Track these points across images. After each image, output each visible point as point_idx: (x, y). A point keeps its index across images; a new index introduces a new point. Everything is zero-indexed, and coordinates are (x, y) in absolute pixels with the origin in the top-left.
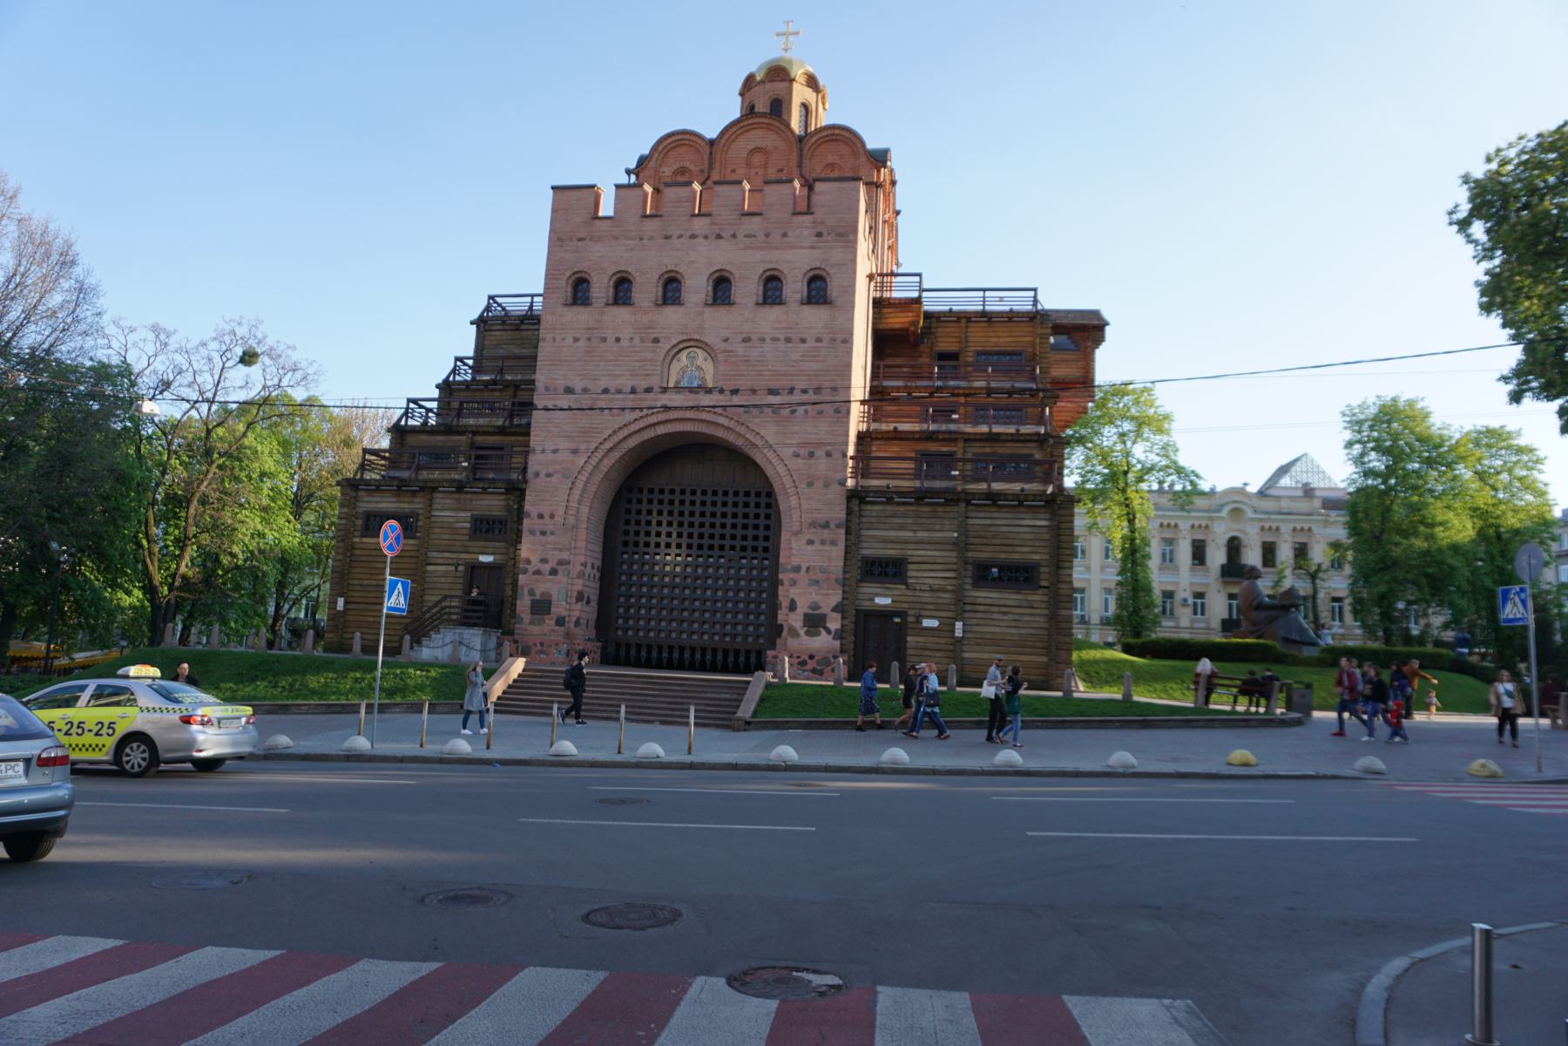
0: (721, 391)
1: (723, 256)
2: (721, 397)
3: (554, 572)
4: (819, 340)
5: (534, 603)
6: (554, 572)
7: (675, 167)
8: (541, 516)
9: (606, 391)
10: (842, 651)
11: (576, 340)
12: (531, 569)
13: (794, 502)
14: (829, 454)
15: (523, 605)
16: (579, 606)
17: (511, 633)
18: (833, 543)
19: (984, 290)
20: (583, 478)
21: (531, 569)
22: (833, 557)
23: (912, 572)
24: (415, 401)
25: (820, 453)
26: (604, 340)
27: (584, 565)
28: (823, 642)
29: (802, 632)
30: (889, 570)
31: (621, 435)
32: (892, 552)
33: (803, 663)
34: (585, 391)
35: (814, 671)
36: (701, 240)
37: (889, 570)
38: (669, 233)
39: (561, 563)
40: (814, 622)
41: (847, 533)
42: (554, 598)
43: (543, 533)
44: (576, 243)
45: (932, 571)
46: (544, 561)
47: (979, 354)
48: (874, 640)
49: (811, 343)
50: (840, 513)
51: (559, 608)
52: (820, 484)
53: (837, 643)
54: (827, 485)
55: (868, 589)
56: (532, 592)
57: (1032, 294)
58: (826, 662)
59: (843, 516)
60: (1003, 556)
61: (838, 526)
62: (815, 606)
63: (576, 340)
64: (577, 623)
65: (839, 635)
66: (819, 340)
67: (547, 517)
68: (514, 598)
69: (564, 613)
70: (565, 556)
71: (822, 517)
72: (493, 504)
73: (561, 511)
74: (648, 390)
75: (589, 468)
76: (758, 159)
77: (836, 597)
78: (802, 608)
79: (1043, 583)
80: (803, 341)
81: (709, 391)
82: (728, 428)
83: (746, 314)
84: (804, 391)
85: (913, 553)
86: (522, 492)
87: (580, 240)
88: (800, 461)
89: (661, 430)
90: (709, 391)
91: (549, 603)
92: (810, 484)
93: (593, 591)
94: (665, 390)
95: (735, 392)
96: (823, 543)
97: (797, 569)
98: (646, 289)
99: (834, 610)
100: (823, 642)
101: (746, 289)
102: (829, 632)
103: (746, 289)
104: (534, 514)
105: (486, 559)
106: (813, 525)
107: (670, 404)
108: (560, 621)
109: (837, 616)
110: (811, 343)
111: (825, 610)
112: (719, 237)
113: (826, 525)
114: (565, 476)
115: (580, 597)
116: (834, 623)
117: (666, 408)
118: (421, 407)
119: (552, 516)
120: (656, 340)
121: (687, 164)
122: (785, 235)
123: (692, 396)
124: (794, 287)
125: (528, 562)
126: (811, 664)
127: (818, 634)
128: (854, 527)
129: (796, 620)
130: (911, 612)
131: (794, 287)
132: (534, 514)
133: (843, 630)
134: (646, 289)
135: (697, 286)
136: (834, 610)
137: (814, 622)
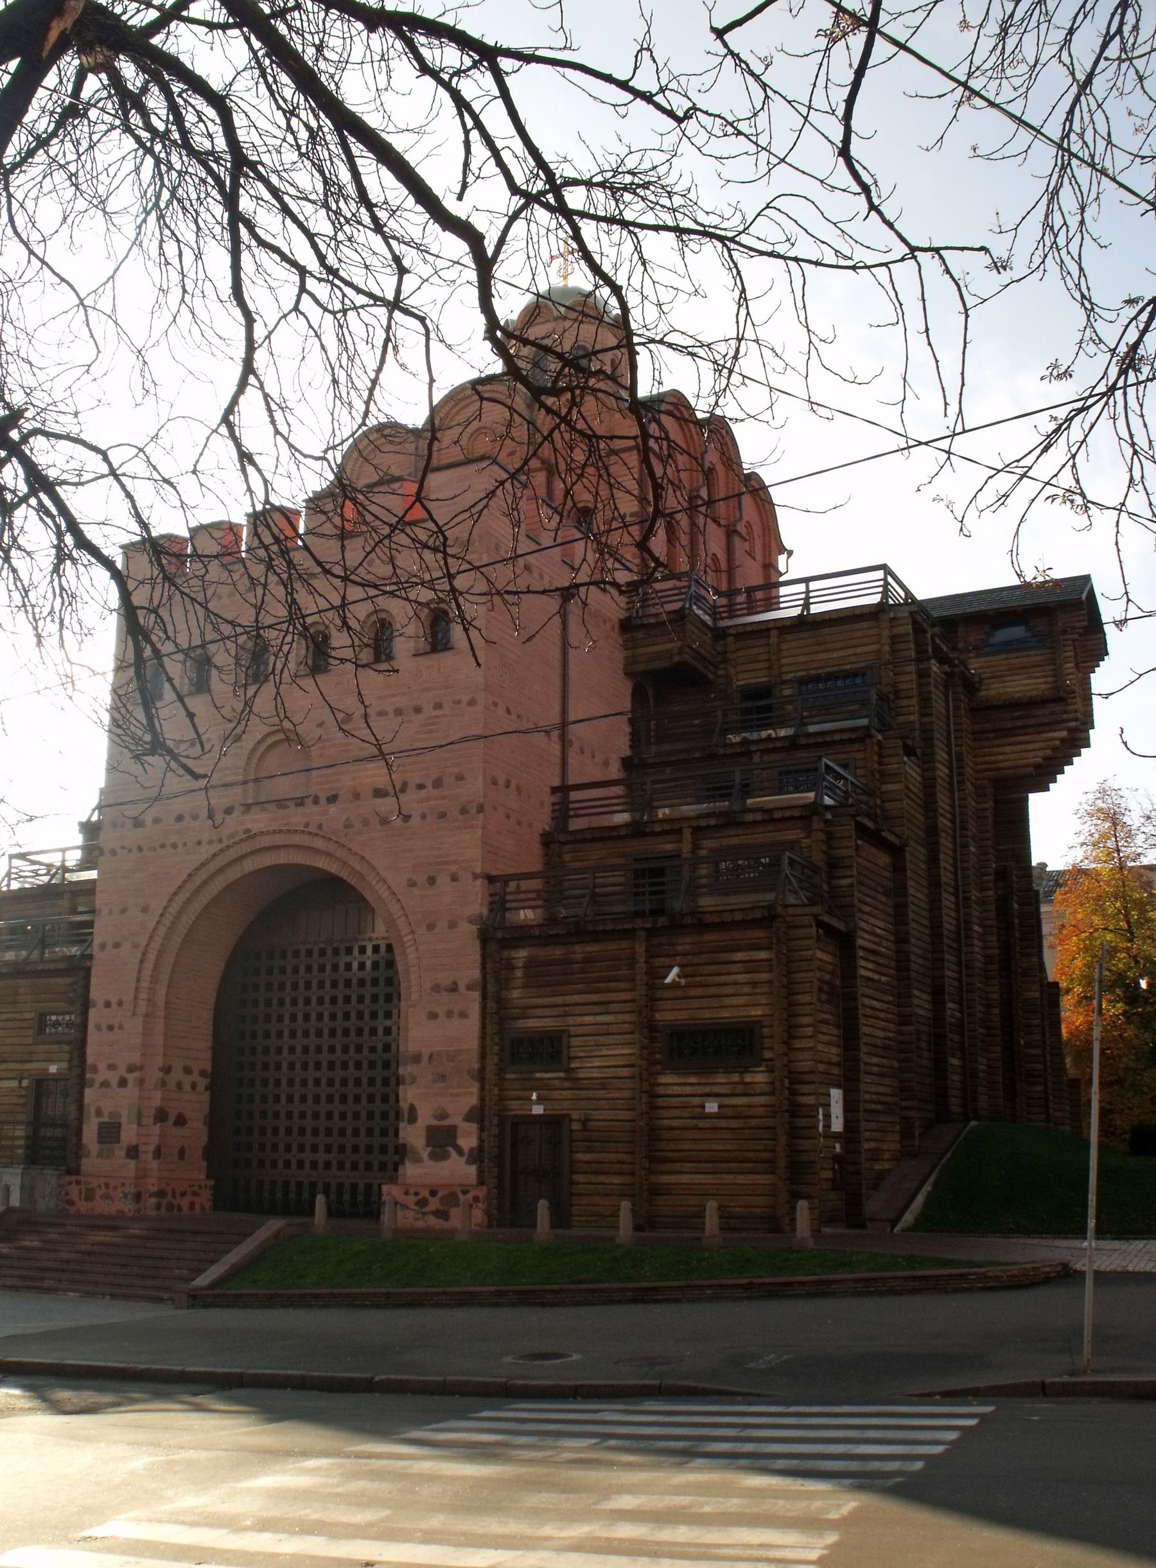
0: (316, 801)
2: (315, 809)
3: (123, 1083)
4: (438, 706)
5: (101, 1126)
6: (123, 1083)
8: (108, 1004)
9: (180, 818)
10: (481, 1182)
12: (99, 1078)
13: (412, 957)
14: (454, 878)
15: (90, 1131)
16: (157, 1129)
17: (76, 1171)
18: (463, 1015)
19: (806, 581)
20: (156, 945)
21: (99, 1078)
24: (23, 856)
25: (443, 881)
27: (167, 1070)
29: (425, 1155)
31: (198, 880)
33: (422, 1203)
34: (156, 821)
35: (437, 1213)
37: (548, 1049)
39: (131, 1069)
40: (441, 1140)
41: (484, 997)
42: (124, 1120)
43: (111, 1028)
45: (605, 1051)
46: (112, 1067)
47: (801, 682)
48: (524, 1162)
49: (428, 711)
50: (469, 966)
51: (129, 1134)
52: (442, 924)
53: (473, 1170)
54: (452, 925)
56: (99, 1113)
57: (880, 574)
58: (451, 1199)
59: (476, 973)
60: (707, 1014)
61: (469, 988)
62: (443, 1116)
64: (158, 1153)
65: (476, 1156)
66: (438, 706)
67: (114, 1005)
68: (80, 1121)
69: (134, 1142)
70: (136, 1058)
71: (446, 979)
73: (128, 997)
75: (162, 930)
78: (425, 1118)
79: (768, 1055)
80: (418, 710)
82: (329, 855)
84: (421, 787)
86: (88, 971)
88: (416, 891)
89: (249, 866)
91: (120, 1124)
92: (431, 927)
93: (196, 1104)
94: (247, 808)
95: (332, 799)
96: (450, 1014)
97: (417, 1059)
99: (468, 1118)
102: (460, 1152)
104: (100, 1003)
105: (53, 1069)
106: (436, 988)
107: (256, 828)
108: (133, 1152)
109: (473, 1127)
110: (428, 711)
111: (456, 1120)
113: (454, 988)
114: (135, 946)
115: (161, 1116)
116: (468, 1139)
117: (250, 836)
118: (33, 863)
123: (281, 812)
125: (95, 1070)
126: (434, 1204)
127: (444, 1156)
128: (491, 989)
130: (575, 1115)
133: (480, 1148)
136: (468, 1118)
137: (441, 1140)
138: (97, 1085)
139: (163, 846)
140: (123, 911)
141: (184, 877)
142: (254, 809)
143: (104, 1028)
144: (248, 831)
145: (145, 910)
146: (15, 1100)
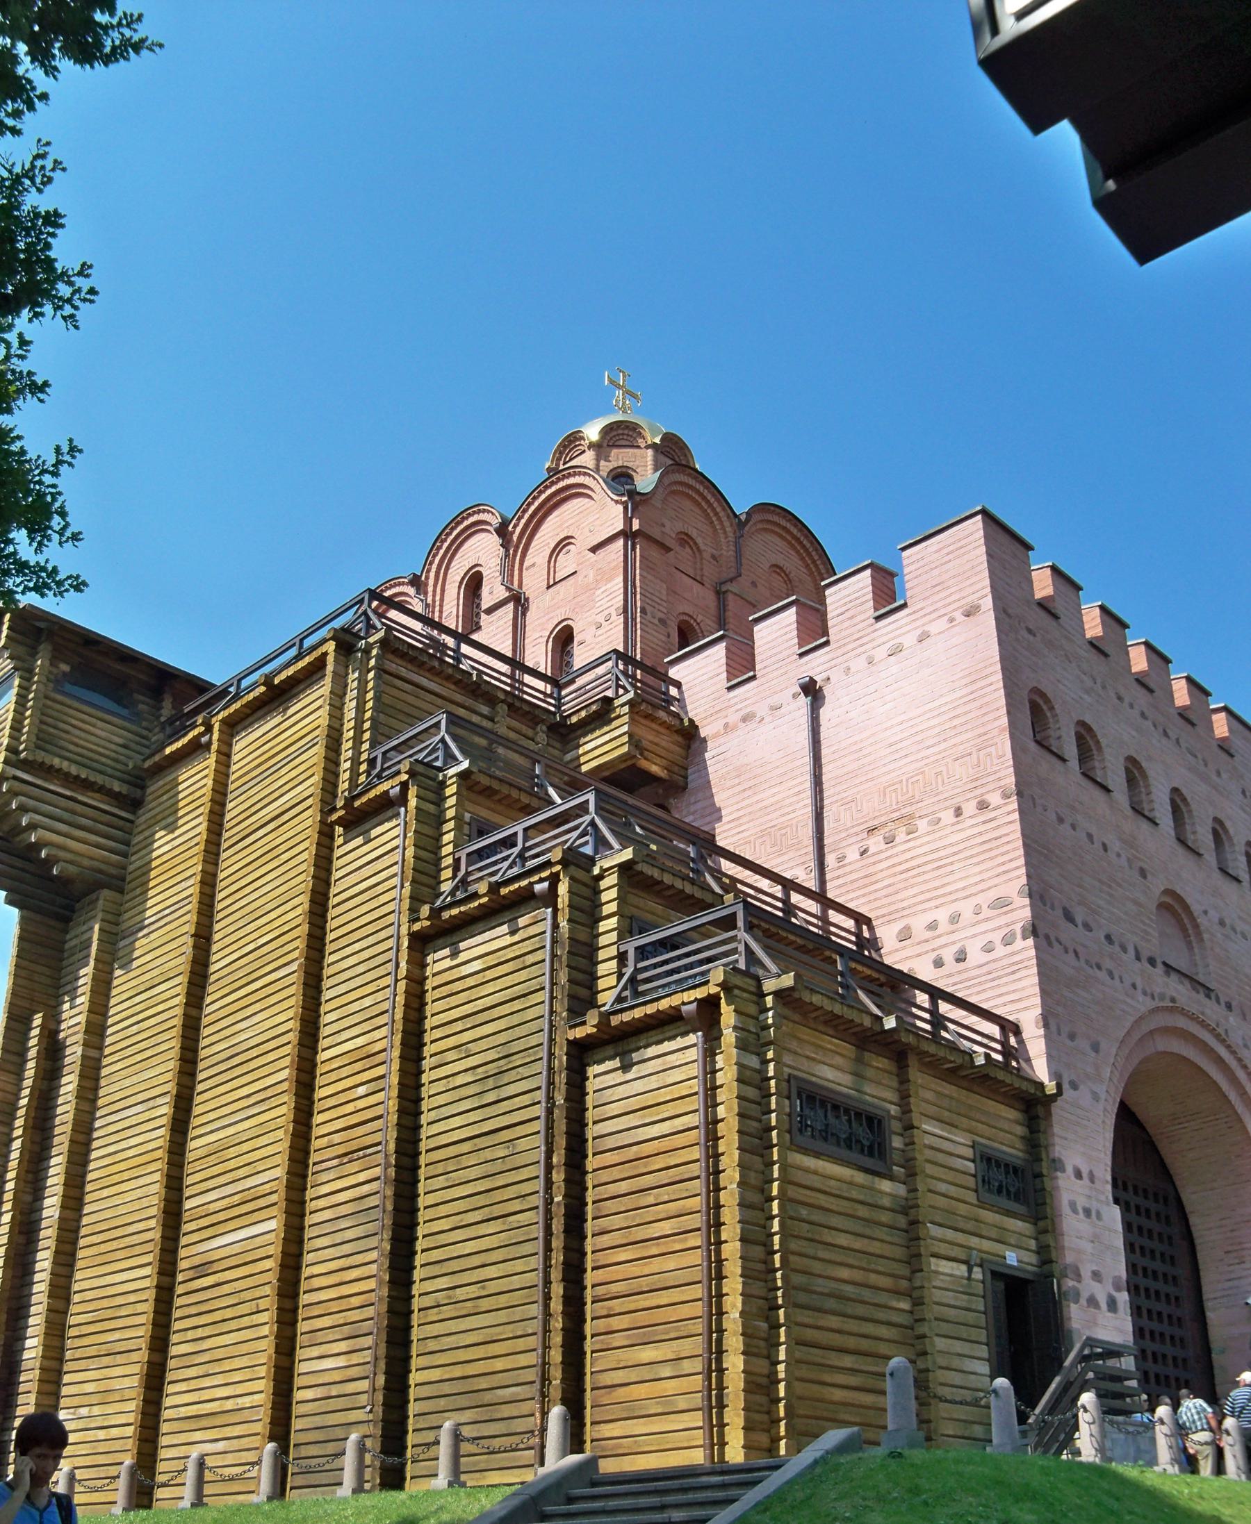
3: (1112, 1305)
7: (679, 526)
8: (1078, 1175)
11: (1061, 820)
26: (1090, 836)
36: (1149, 724)
38: (1122, 692)
43: (1087, 1212)
44: (1024, 633)
46: (1096, 1276)
63: (1061, 820)
72: (1004, 1130)
74: (1152, 962)
81: (1208, 992)
87: (1030, 631)
90: (1208, 992)
104: (1070, 1170)
105: (1012, 1258)
112: (1165, 734)
114: (1096, 1097)
119: (1092, 1178)
120: (1143, 873)
121: (694, 534)
122: (1218, 774)
132: (1070, 1170)
138: (1083, 1301)
139: (1099, 968)
140: (1072, 1037)
141: (1128, 1025)
142: (1174, 976)
143: (1081, 1211)
144: (1173, 1000)
145: (1096, 1048)
146: (963, 1300)
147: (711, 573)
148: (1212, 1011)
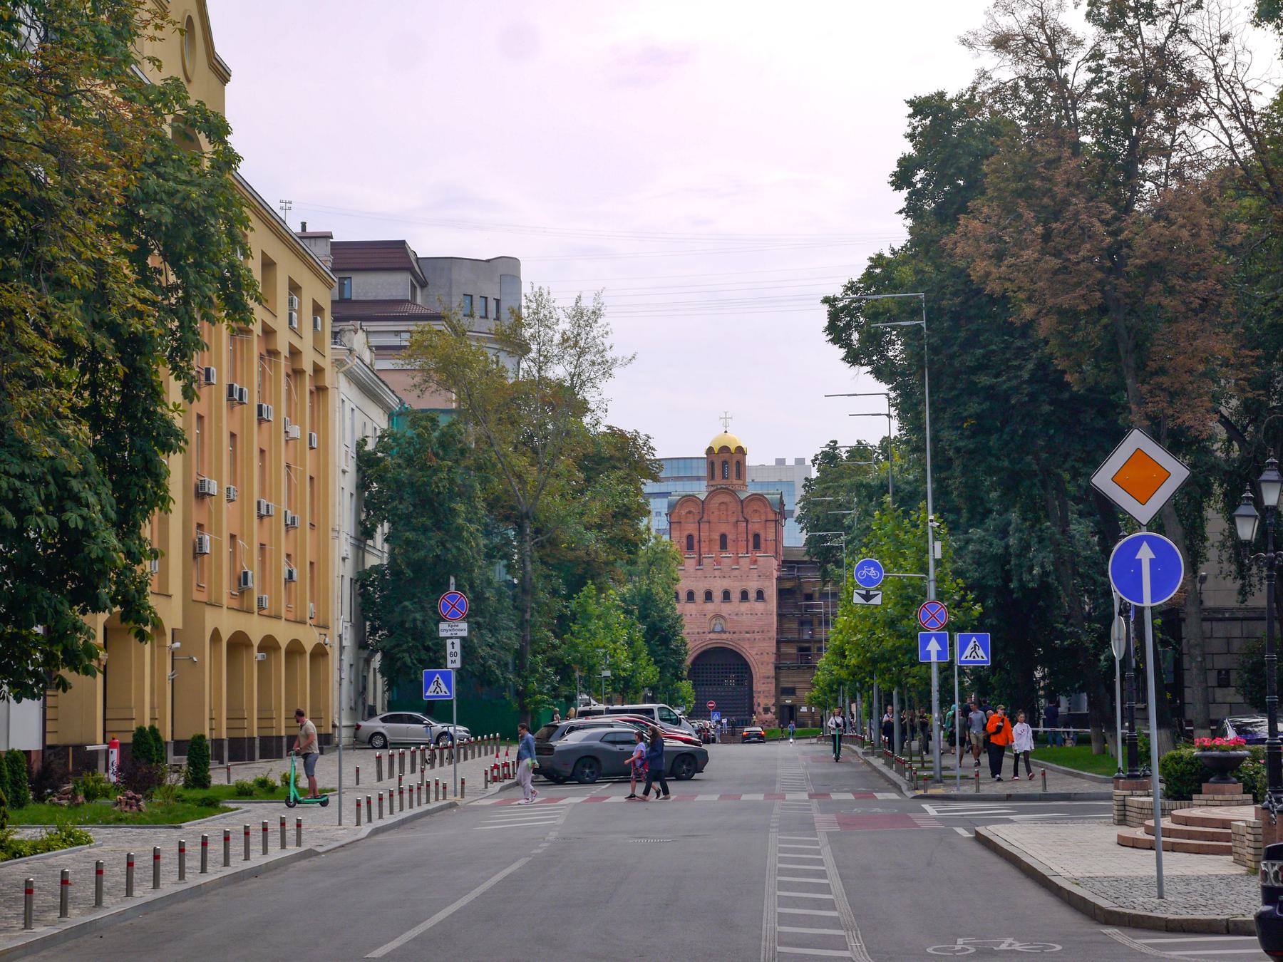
1: (726, 584)
22: (772, 687)
23: (798, 692)
28: (770, 716)
30: (791, 691)
32: (790, 685)
37: (791, 691)
50: (772, 673)
55: (783, 698)
76: (723, 507)
77: (773, 701)
83: (735, 606)
85: (798, 685)
98: (700, 596)
100: (770, 716)
101: (735, 596)
103: (735, 596)
116: (773, 710)
124: (752, 595)
129: (761, 710)
131: (752, 595)
134: (700, 596)
135: (718, 595)
137: (766, 710)
147: (697, 518)
148: (725, 636)
